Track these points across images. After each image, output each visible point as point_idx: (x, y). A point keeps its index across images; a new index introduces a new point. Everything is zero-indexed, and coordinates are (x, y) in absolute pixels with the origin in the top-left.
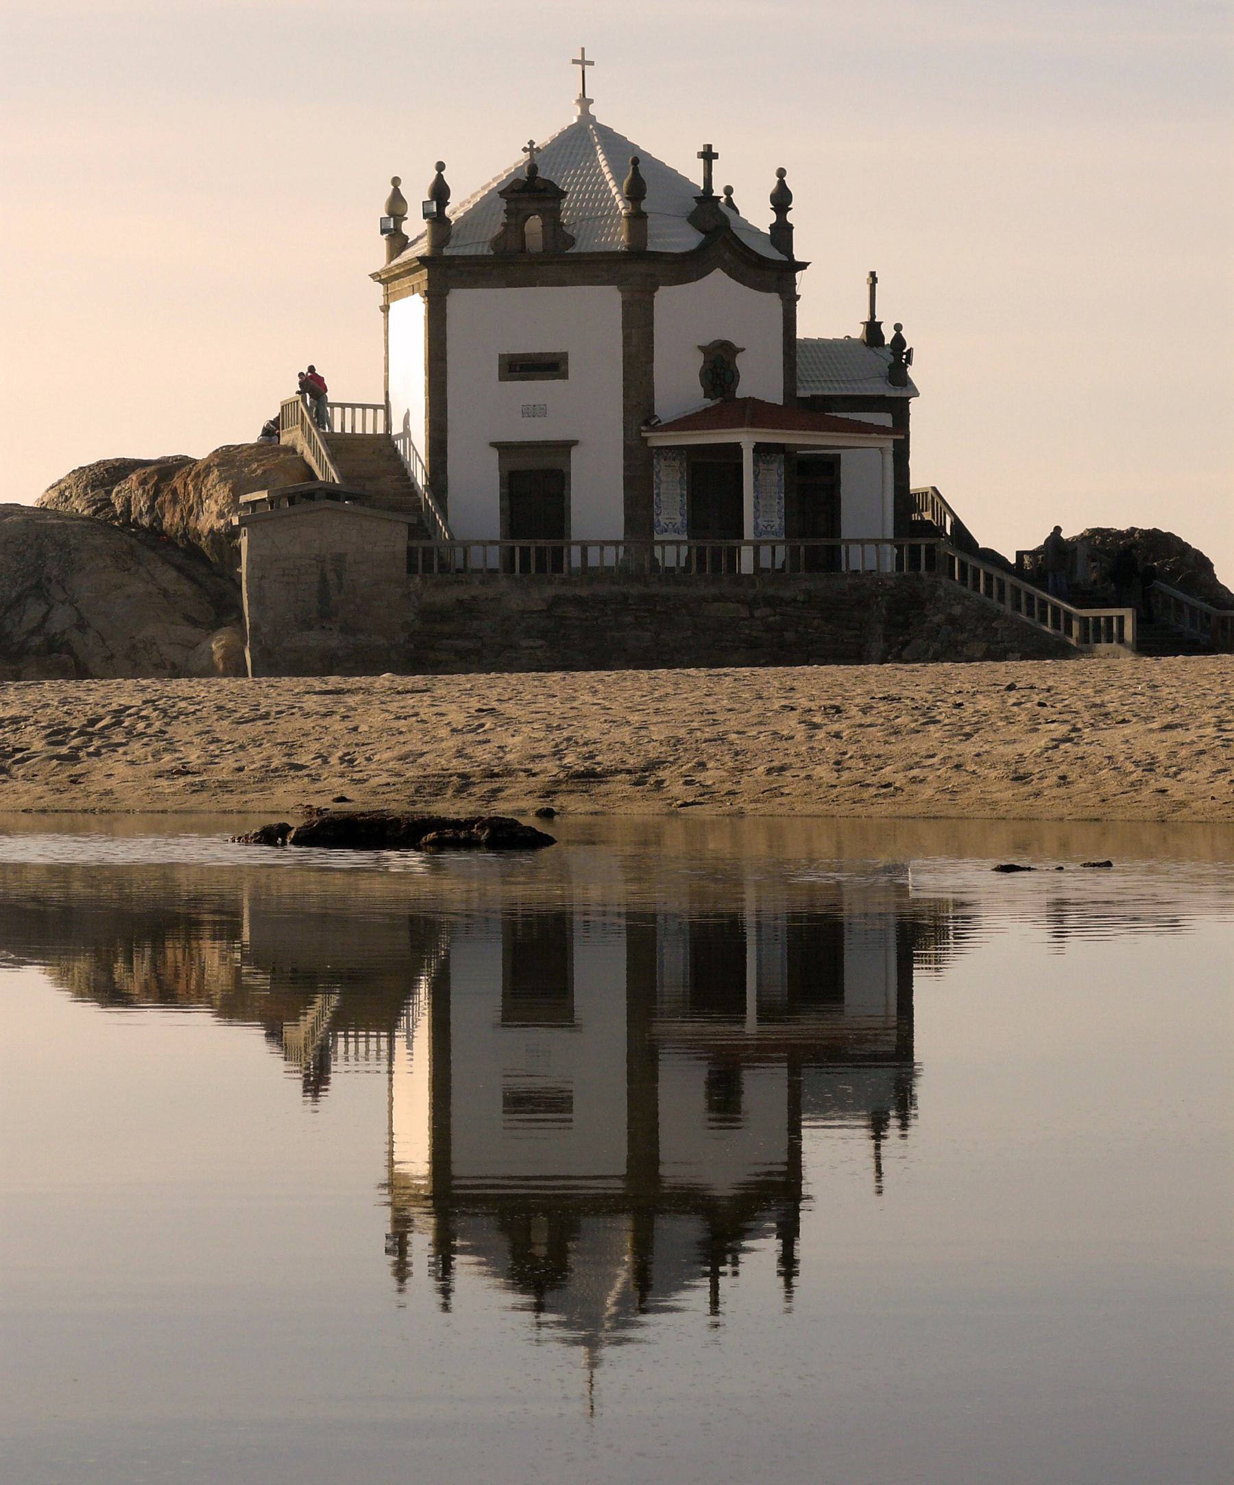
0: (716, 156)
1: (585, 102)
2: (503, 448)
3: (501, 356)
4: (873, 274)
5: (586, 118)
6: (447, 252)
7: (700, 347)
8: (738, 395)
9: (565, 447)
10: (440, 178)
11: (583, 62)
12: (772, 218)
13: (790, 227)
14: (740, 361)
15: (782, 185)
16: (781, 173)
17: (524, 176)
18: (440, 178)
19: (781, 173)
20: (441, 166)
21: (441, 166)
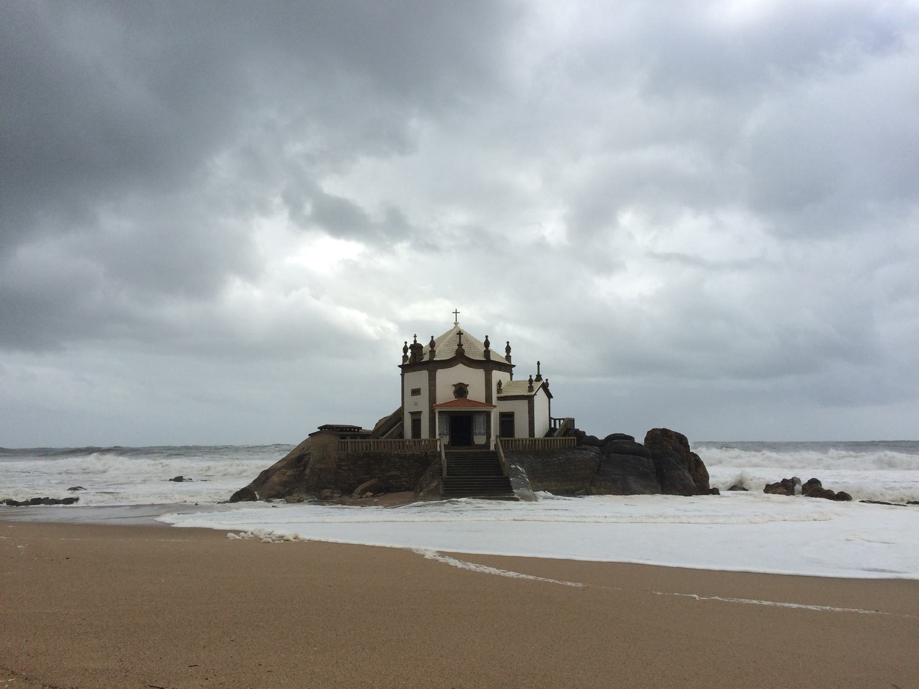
0: (462, 334)
1: (456, 323)
2: (412, 414)
3: (412, 390)
4: (538, 362)
6: (405, 363)
7: (453, 385)
8: (468, 398)
9: (420, 413)
10: (406, 345)
11: (456, 313)
12: (485, 349)
13: (490, 351)
14: (468, 388)
15: (487, 340)
16: (487, 337)
17: (413, 343)
18: (406, 345)
19: (487, 337)
20: (406, 343)
21: (406, 343)
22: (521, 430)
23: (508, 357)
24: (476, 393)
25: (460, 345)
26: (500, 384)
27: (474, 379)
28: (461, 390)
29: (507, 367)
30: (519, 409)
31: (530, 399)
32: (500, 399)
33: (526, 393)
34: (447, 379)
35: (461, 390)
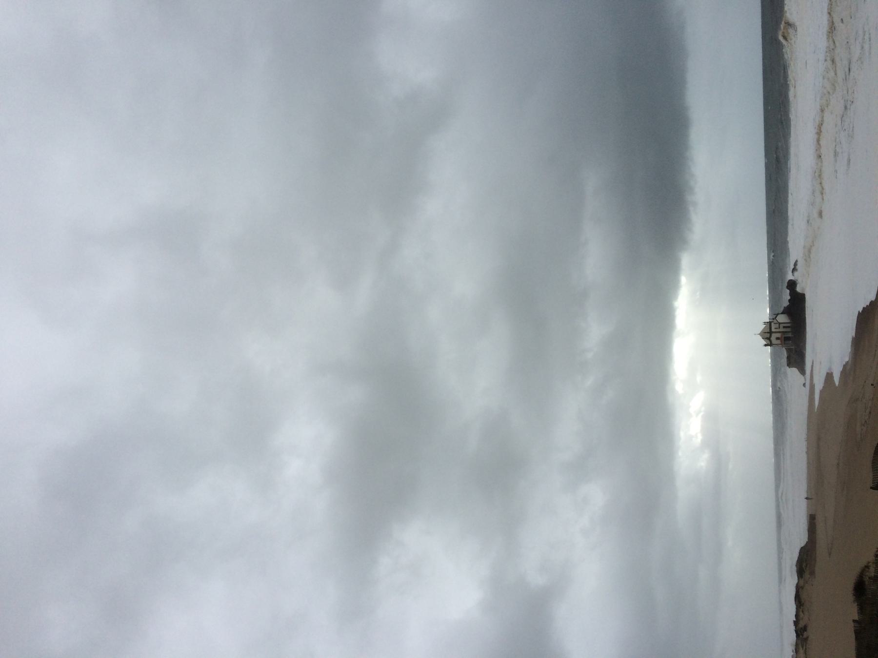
5: (760, 334)
22: (789, 325)
23: (767, 322)
24: (779, 335)
25: (766, 338)
26: (776, 328)
27: (774, 336)
28: (778, 339)
29: (770, 323)
30: (782, 326)
31: (780, 323)
32: (779, 327)
33: (778, 325)
34: (774, 341)
35: (778, 339)
